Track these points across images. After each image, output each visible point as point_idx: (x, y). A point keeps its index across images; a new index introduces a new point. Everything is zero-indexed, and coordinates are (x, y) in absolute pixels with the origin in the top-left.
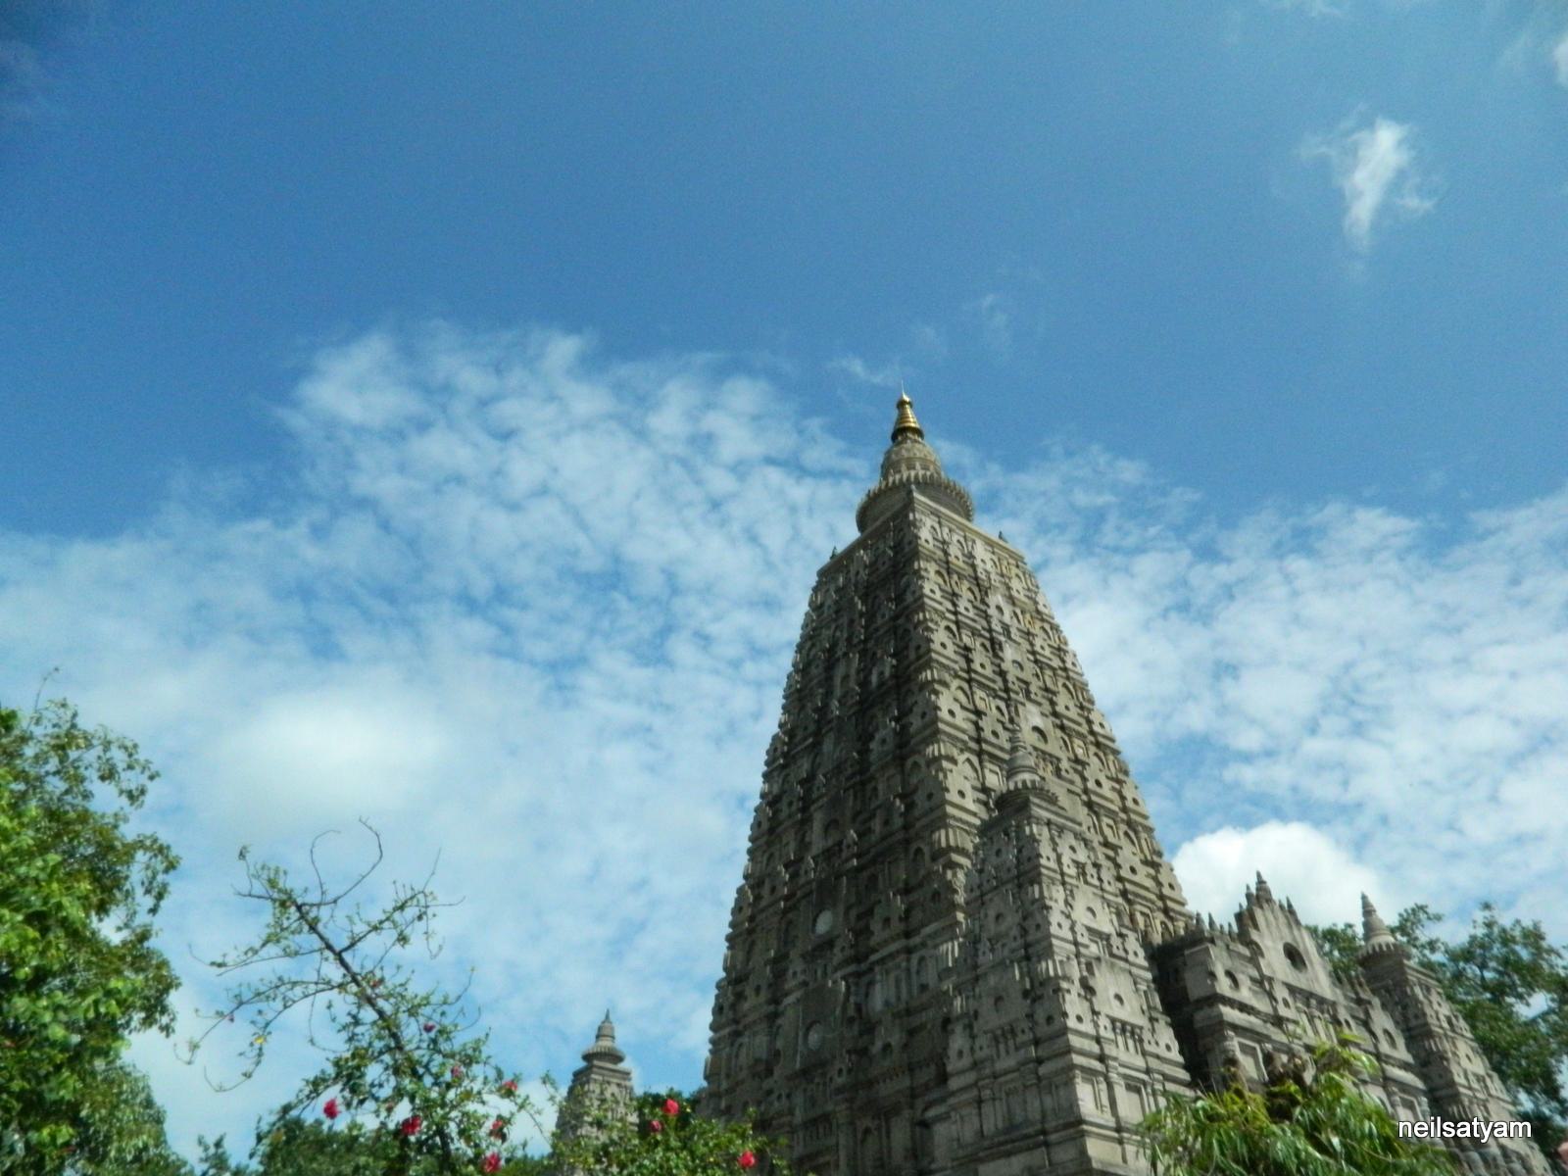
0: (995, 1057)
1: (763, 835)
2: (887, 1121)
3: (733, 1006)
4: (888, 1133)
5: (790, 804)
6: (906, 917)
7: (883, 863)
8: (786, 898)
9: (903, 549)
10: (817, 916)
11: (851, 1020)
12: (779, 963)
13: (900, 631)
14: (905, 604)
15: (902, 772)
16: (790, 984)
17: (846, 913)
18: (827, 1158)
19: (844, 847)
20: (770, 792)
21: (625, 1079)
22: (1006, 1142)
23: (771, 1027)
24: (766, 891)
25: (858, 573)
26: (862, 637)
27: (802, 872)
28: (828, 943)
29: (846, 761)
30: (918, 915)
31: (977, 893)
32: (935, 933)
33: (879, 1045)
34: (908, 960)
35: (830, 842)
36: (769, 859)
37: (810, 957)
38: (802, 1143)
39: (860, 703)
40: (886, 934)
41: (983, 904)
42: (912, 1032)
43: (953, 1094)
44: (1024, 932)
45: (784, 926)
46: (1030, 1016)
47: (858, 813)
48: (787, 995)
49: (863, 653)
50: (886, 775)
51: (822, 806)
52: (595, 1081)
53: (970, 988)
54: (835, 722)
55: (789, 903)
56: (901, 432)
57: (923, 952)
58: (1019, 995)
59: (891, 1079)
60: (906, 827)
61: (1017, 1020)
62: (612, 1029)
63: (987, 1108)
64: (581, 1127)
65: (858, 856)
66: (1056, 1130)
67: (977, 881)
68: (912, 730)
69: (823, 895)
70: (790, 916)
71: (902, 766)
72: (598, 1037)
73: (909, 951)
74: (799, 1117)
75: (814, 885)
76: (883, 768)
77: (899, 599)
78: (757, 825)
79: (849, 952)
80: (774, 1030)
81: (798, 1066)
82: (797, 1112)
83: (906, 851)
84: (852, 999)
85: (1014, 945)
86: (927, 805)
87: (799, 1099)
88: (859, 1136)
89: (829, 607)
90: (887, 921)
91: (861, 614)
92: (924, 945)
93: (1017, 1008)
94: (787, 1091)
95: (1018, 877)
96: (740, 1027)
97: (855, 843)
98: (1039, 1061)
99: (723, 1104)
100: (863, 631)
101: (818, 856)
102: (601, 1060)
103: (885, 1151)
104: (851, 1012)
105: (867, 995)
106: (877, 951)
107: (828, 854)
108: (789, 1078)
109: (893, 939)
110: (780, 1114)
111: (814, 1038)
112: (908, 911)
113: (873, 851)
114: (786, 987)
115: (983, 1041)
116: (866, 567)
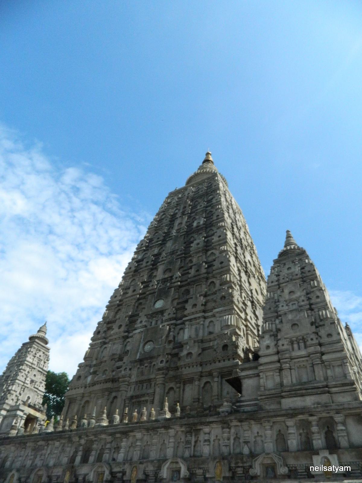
0: (291, 350)
1: (131, 272)
2: (184, 385)
3: (105, 332)
4: (184, 390)
5: (147, 262)
6: (205, 305)
7: (194, 285)
8: (140, 294)
9: (212, 187)
10: (156, 301)
11: (170, 342)
12: (133, 319)
13: (208, 212)
14: (212, 203)
15: (206, 255)
16: (138, 325)
17: (173, 301)
18: (147, 398)
19: (174, 277)
20: (137, 258)
21: (47, 351)
22: (300, 389)
23: (124, 342)
24: (130, 292)
25: (189, 194)
26: (189, 212)
27: (150, 285)
28: (161, 312)
29: (178, 250)
30: (210, 305)
31: (276, 283)
32: (222, 311)
33: (185, 352)
34: (204, 321)
35: (166, 276)
36: (132, 281)
37: (151, 316)
38: (132, 389)
39: (187, 232)
40: (194, 310)
41: (279, 288)
42: (204, 350)
43: (261, 365)
44: (309, 299)
45: (136, 305)
46: (317, 333)
47: (182, 267)
48: (135, 329)
49: (189, 217)
50: (197, 256)
51: (163, 264)
52: (34, 348)
53: (273, 320)
54: (173, 237)
55: (141, 296)
56: (207, 161)
57: (212, 319)
58: (309, 325)
59: (189, 367)
60: (208, 273)
61: (308, 334)
62: (46, 330)
63: (285, 373)
64: (23, 365)
65: (181, 282)
66: (336, 386)
67: (276, 278)
68: (213, 241)
69: (162, 294)
70: (141, 301)
71: (206, 253)
72: (39, 331)
73: (205, 318)
74: (134, 379)
75: (157, 290)
76: (197, 253)
77: (209, 201)
78: (129, 268)
79: (172, 316)
80: (125, 343)
81: (138, 357)
82: (133, 377)
83: (206, 281)
84: (171, 333)
85: (303, 303)
86: (220, 266)
87: (135, 372)
88: (166, 391)
89: (174, 203)
90: (195, 305)
91: (190, 205)
92: (214, 316)
93: (306, 329)
94: (130, 367)
95: (302, 278)
96: (107, 341)
97: (180, 277)
98: (323, 354)
99: (92, 371)
100: (190, 210)
101: (159, 280)
102: (37, 341)
103: (181, 398)
104: (171, 338)
105: (178, 334)
106: (187, 316)
107: (164, 281)
108: (131, 362)
109: (196, 312)
110: (124, 377)
111: (148, 347)
112: (206, 303)
113: (189, 280)
114: (136, 326)
115: (285, 342)
116: (193, 192)
